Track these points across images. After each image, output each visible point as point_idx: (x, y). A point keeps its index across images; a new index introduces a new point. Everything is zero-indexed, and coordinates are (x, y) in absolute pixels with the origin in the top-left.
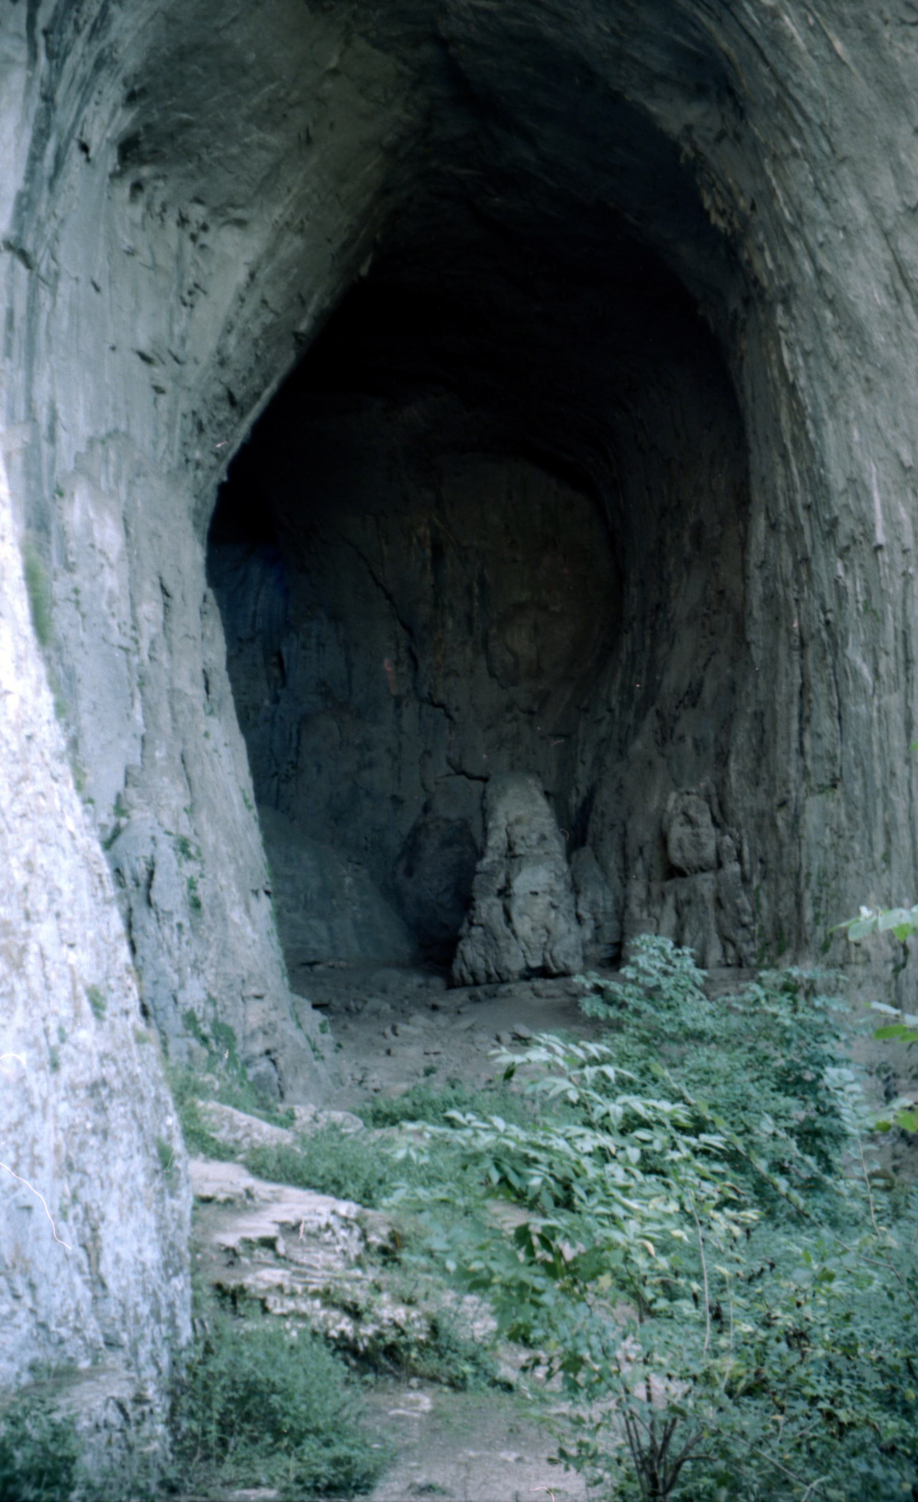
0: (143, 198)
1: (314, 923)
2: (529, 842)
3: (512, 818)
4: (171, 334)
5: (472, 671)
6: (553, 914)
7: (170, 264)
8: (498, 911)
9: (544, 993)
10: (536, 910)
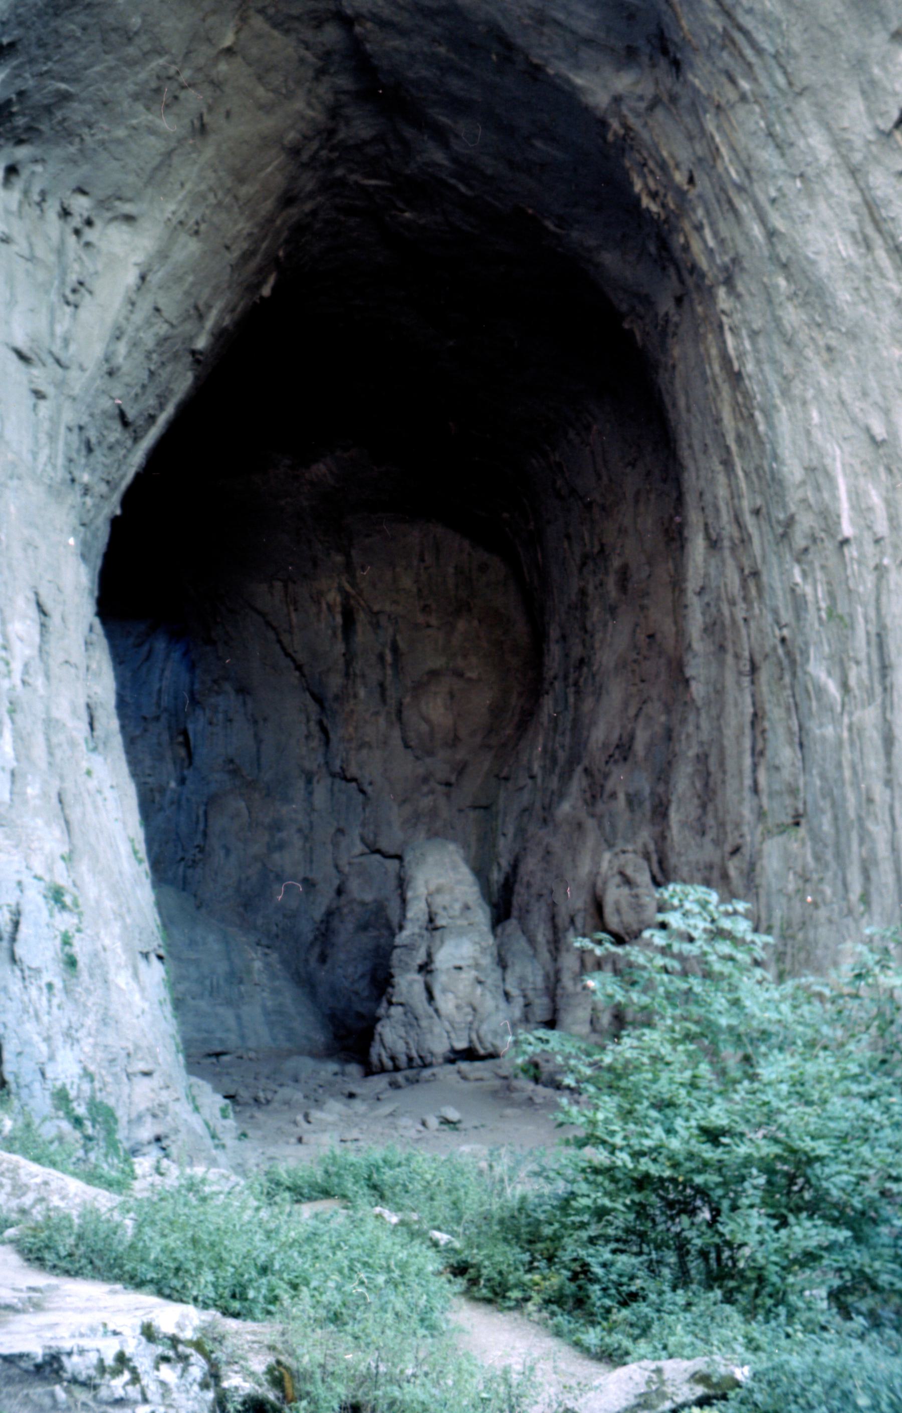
0: (19, 183)
2: (452, 913)
3: (432, 887)
4: (52, 334)
5: (385, 743)
6: (479, 990)
7: (52, 258)
8: (419, 989)
9: (472, 1076)
10: (461, 987)
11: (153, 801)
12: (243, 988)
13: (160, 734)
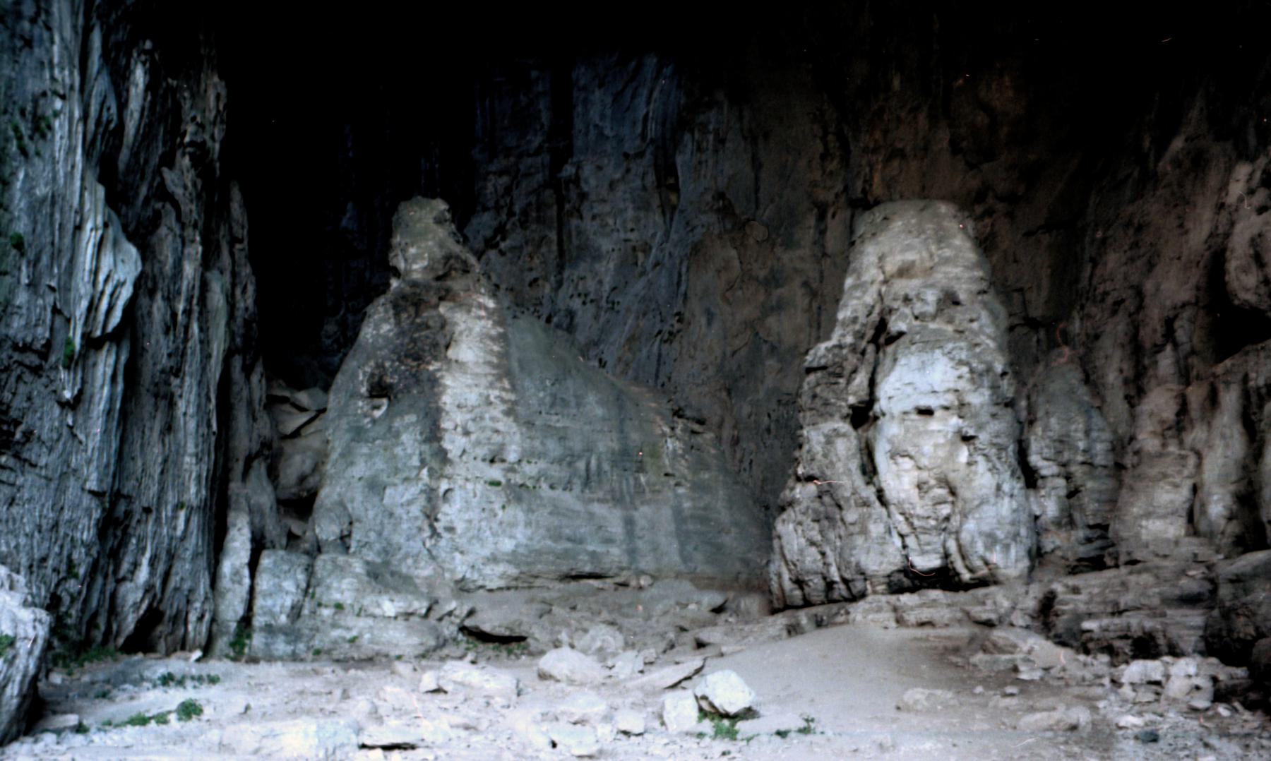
1: (597, 508)
3: (891, 267)
5: (926, 149)
6: (963, 454)
9: (911, 617)
10: (928, 448)
11: (636, 264)
12: (643, 479)
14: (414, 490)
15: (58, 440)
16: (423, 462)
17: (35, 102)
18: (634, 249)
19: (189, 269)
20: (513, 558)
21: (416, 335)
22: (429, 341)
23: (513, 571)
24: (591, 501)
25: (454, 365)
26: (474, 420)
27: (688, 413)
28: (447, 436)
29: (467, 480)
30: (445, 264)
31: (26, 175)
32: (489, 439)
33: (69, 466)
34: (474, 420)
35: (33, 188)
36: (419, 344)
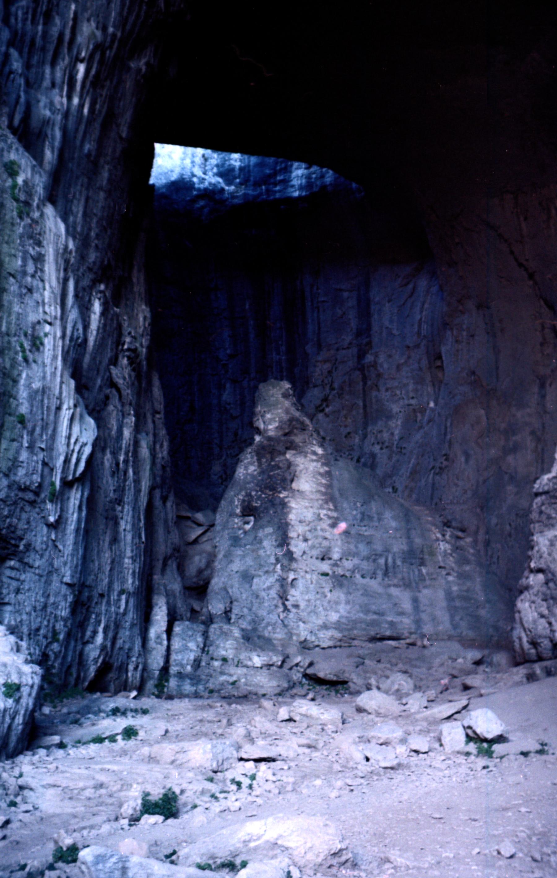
1: (394, 591)
11: (416, 421)
12: (424, 570)
13: (420, 360)
14: (272, 579)
15: (46, 550)
16: (278, 560)
17: (33, 328)
18: (414, 410)
19: (127, 433)
20: (338, 626)
21: (272, 473)
22: (280, 477)
23: (338, 635)
24: (389, 586)
25: (297, 493)
26: (310, 531)
27: (454, 524)
28: (293, 542)
29: (306, 572)
30: (290, 425)
31: (27, 375)
32: (320, 544)
33: (53, 567)
34: (310, 531)
35: (30, 384)
36: (274, 479)
